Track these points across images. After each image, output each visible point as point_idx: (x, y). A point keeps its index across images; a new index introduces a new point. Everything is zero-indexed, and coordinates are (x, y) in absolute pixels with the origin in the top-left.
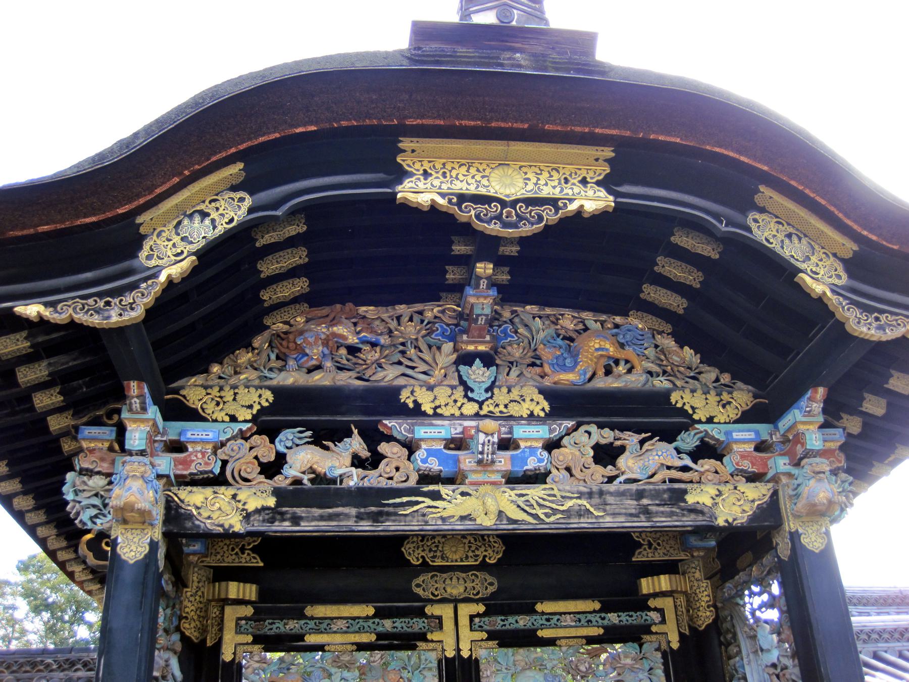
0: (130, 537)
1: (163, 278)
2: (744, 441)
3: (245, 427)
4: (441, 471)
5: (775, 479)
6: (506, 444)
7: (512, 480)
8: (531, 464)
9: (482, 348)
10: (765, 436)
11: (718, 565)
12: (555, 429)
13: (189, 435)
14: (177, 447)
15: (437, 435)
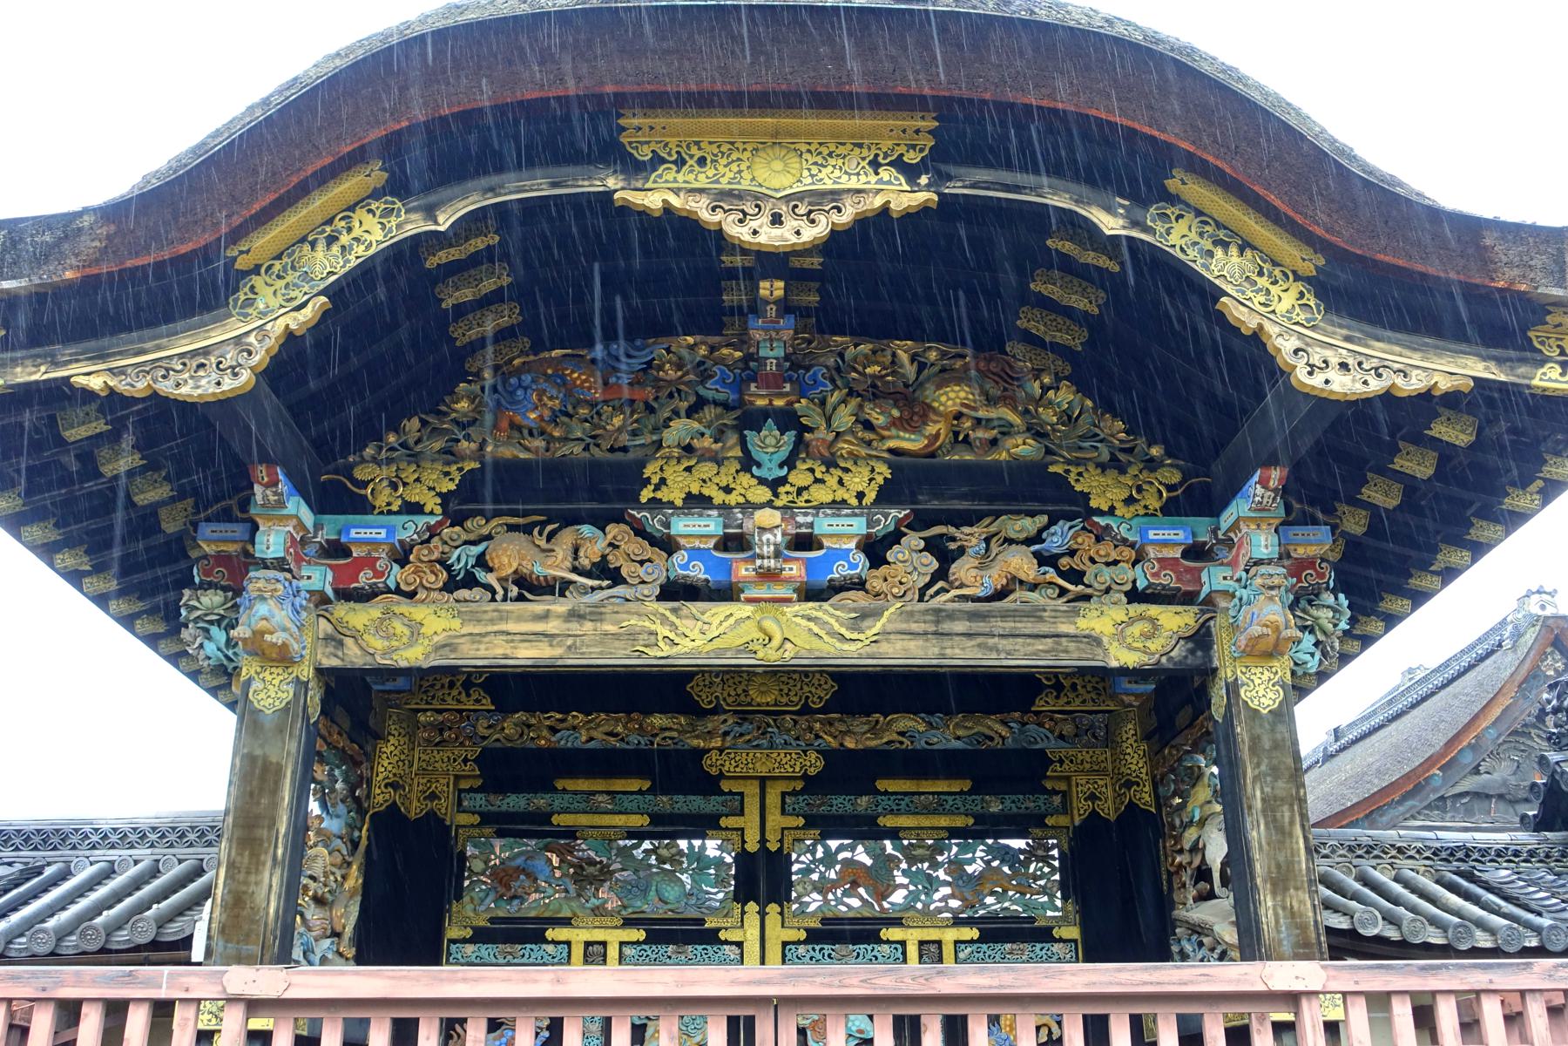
0: (269, 678)
1: (277, 329)
2: (1165, 544)
3: (433, 520)
4: (707, 581)
5: (1209, 602)
6: (804, 542)
7: (812, 593)
8: (840, 571)
9: (779, 403)
10: (1204, 537)
11: (1153, 722)
12: (879, 521)
13: (353, 533)
14: (336, 550)
15: (704, 531)
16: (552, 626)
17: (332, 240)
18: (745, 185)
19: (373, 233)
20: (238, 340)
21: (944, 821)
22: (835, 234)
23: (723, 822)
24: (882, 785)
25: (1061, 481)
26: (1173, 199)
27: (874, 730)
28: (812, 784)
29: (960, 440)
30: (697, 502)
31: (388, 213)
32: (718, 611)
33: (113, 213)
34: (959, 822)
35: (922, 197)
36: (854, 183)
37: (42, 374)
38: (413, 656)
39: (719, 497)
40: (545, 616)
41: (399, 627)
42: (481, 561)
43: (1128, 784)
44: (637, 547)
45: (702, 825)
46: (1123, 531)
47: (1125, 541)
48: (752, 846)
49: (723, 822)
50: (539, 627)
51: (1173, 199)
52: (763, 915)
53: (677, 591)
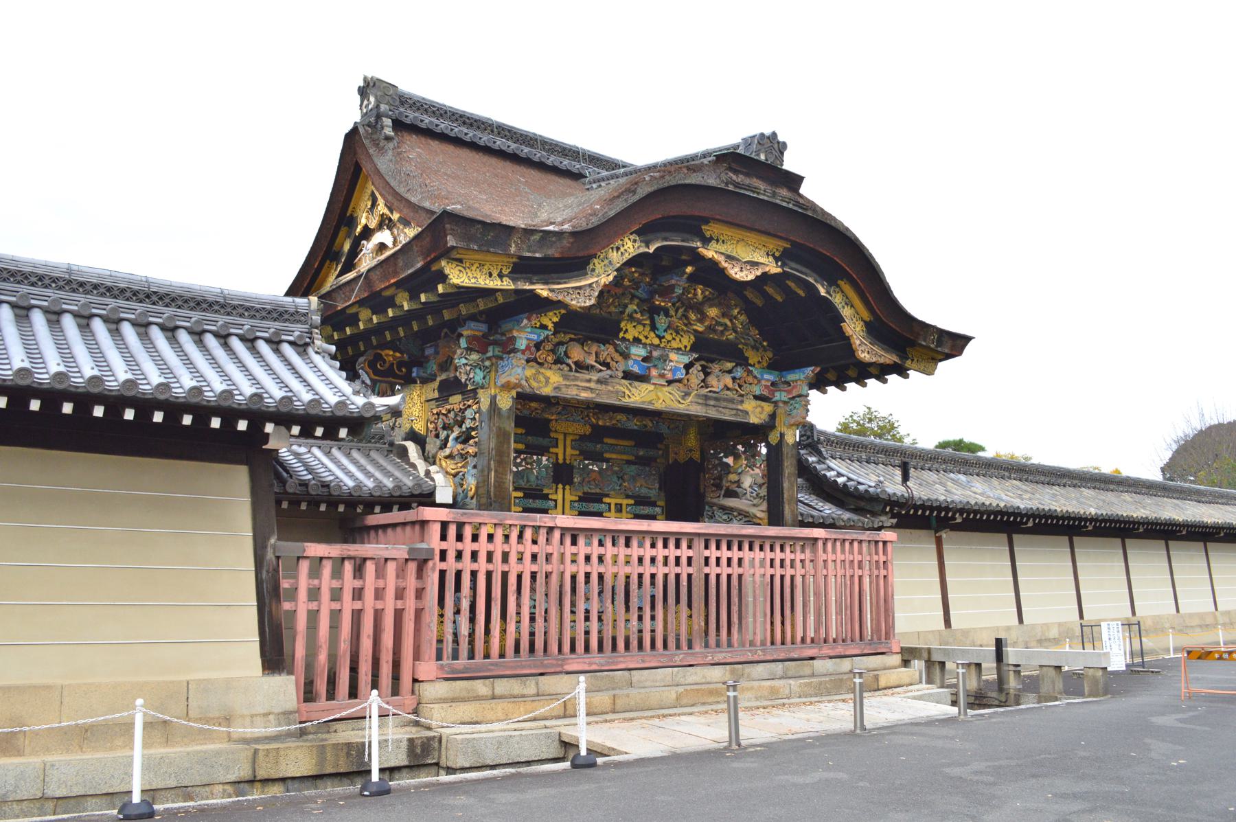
16: (592, 385)
17: (618, 249)
18: (734, 254)
19: (631, 247)
20: (590, 285)
21: (625, 457)
22: (757, 277)
23: (552, 450)
24: (607, 440)
25: (741, 351)
26: (838, 286)
27: (611, 419)
28: (583, 438)
29: (710, 329)
30: (637, 341)
31: (635, 241)
32: (644, 387)
33: (574, 234)
34: (631, 458)
35: (779, 270)
36: (761, 260)
37: (527, 287)
38: (547, 391)
39: (644, 340)
40: (589, 381)
41: (543, 379)
42: (566, 353)
43: (691, 451)
44: (617, 357)
45: (542, 451)
46: (755, 373)
47: (755, 377)
48: (561, 461)
49: (552, 450)
50: (587, 385)
51: (838, 286)
52: (564, 489)
53: (628, 375)
